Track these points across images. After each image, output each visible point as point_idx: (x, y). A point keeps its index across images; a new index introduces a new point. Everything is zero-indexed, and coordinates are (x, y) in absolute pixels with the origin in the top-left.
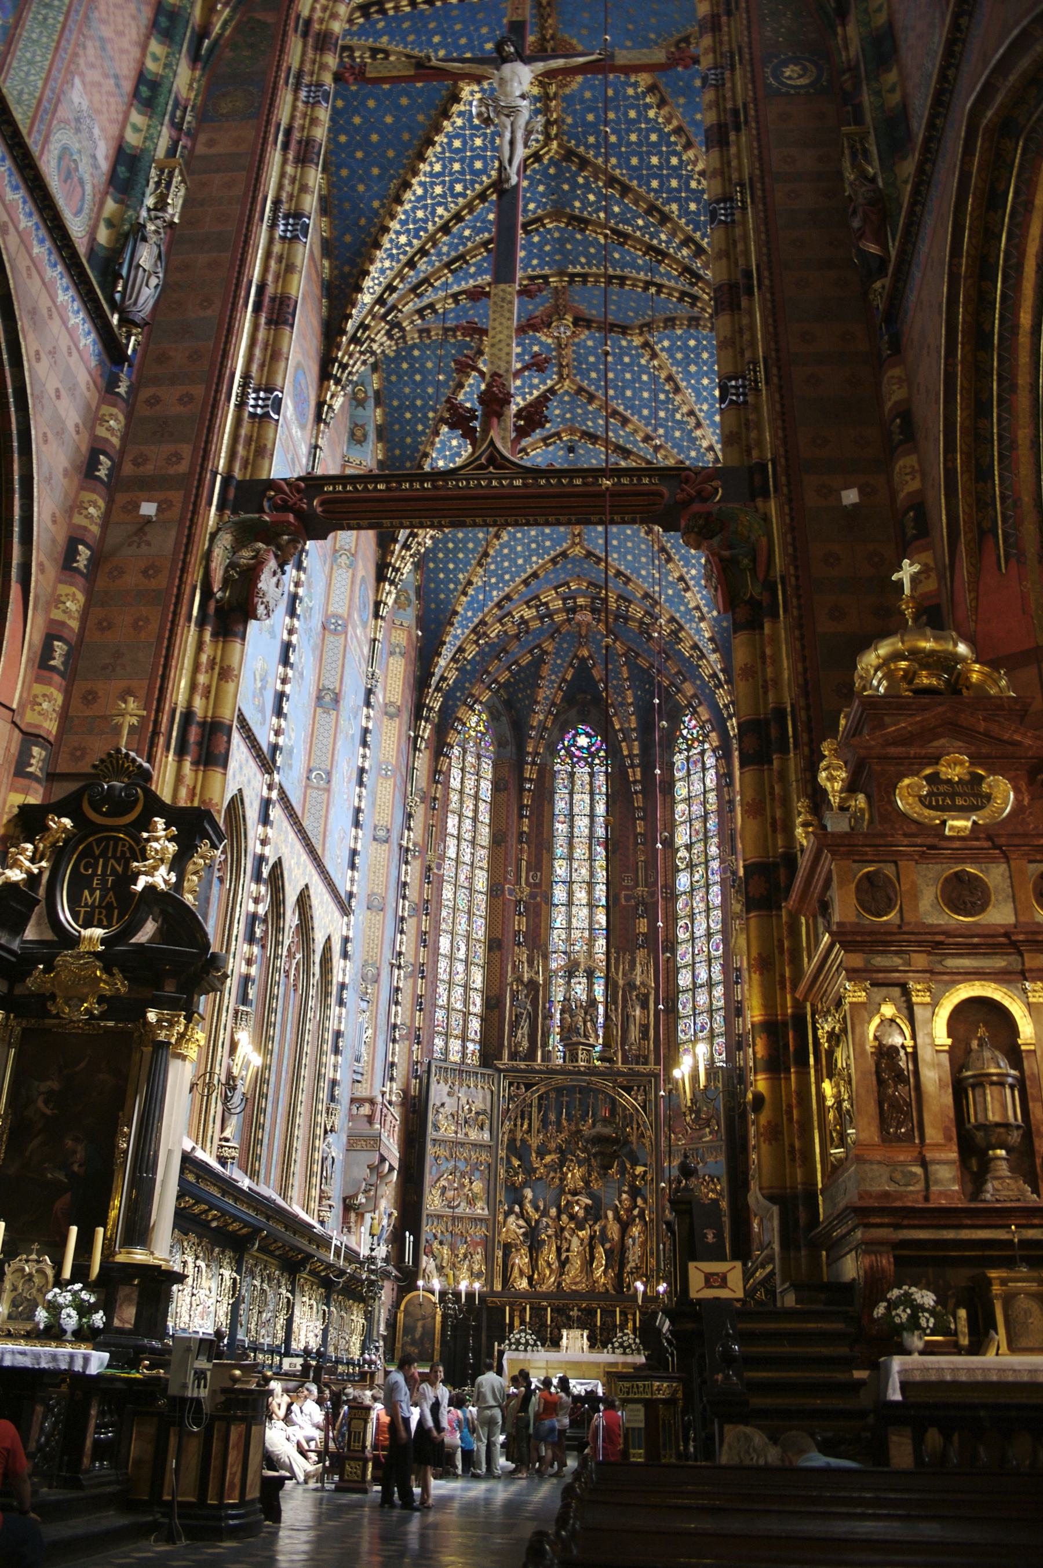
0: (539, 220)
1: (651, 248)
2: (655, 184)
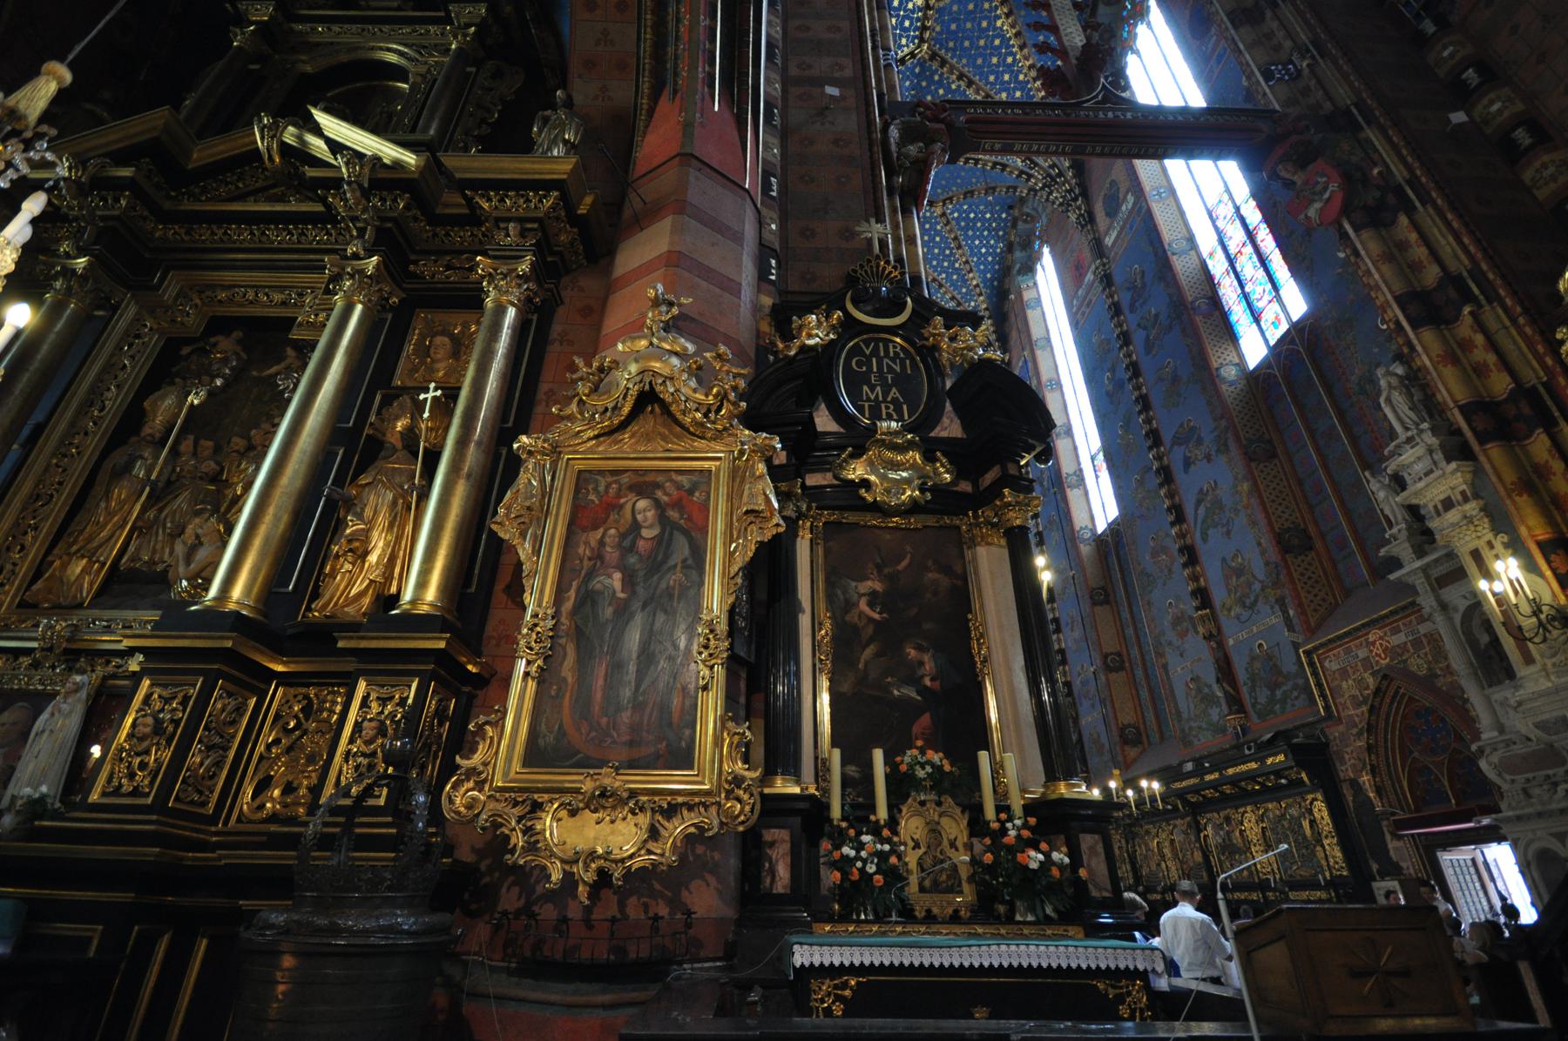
2: (992, 78)
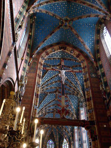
0: (57, 81)
1: (70, 86)
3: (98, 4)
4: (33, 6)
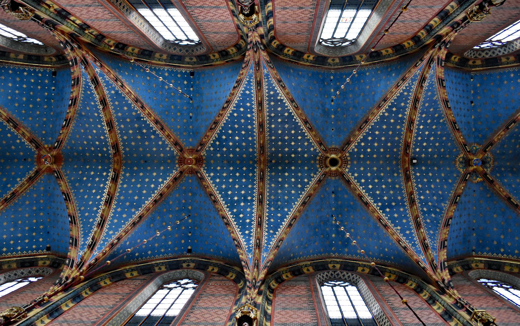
3: (406, 87)
4: (430, 271)
